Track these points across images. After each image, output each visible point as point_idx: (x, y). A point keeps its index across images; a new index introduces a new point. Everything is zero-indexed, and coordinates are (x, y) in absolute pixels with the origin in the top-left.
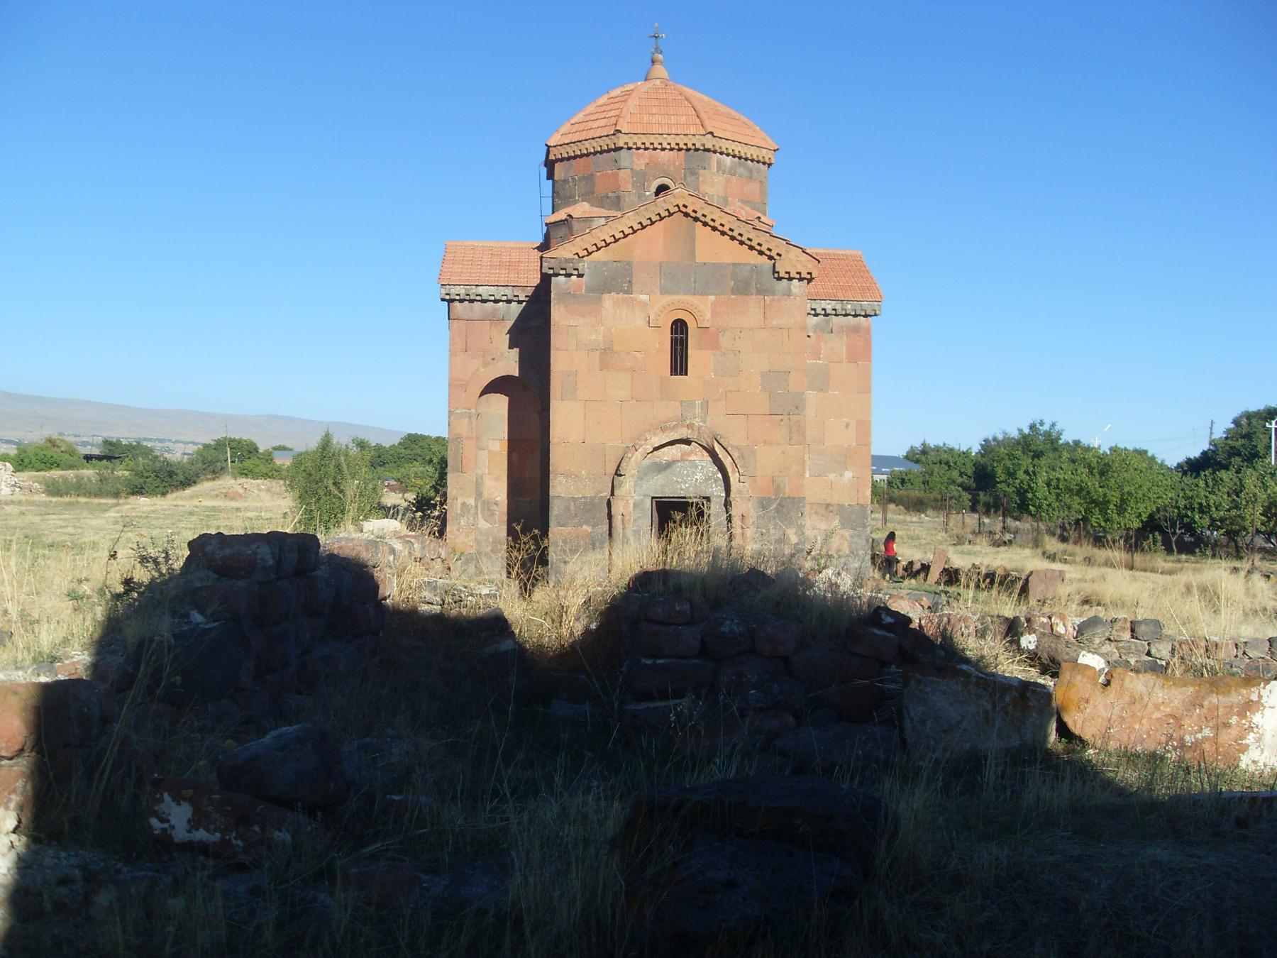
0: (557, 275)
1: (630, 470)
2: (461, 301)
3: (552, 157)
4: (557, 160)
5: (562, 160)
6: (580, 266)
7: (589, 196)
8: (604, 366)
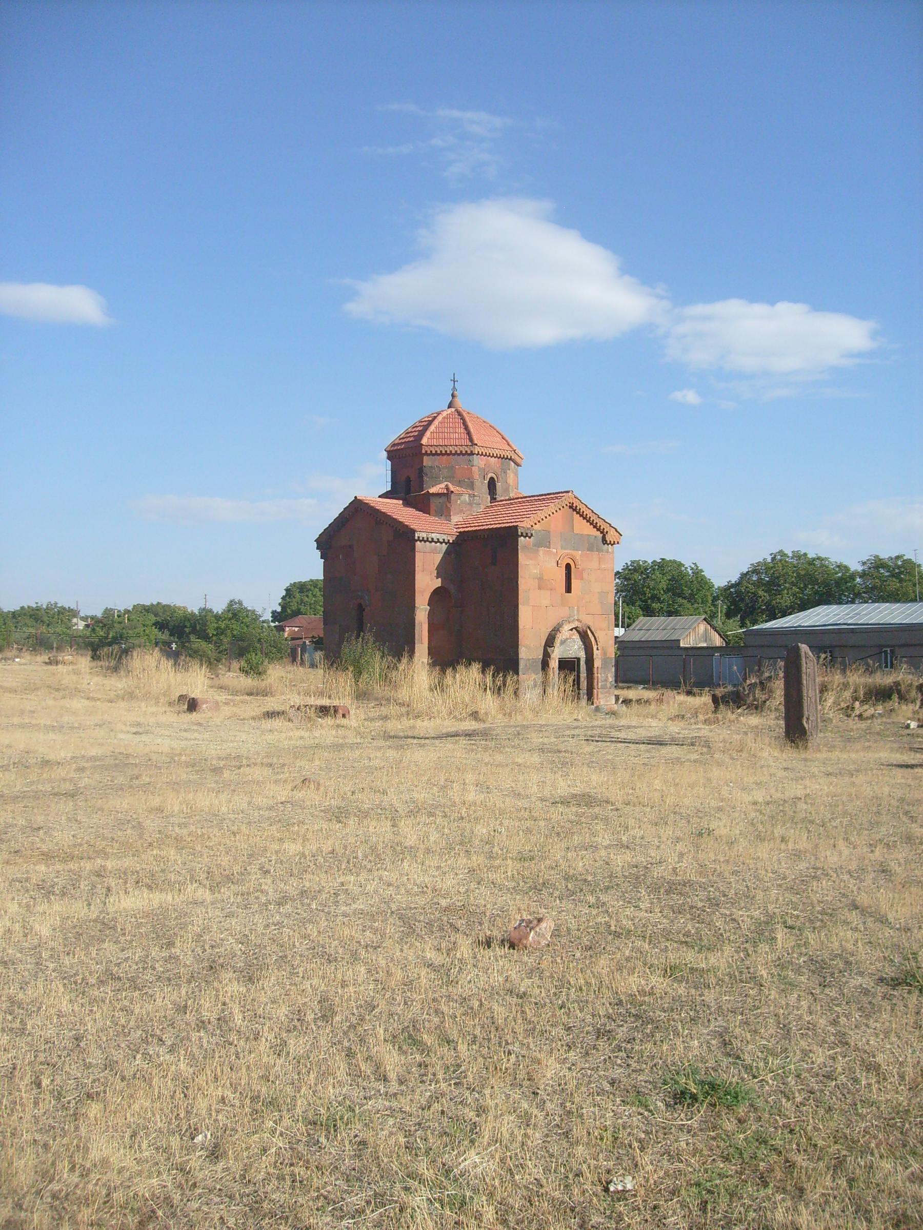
0: (522, 535)
1: (557, 643)
2: (421, 541)
3: (423, 452)
4: (426, 454)
5: (431, 454)
6: (533, 532)
7: (450, 478)
8: (540, 588)
